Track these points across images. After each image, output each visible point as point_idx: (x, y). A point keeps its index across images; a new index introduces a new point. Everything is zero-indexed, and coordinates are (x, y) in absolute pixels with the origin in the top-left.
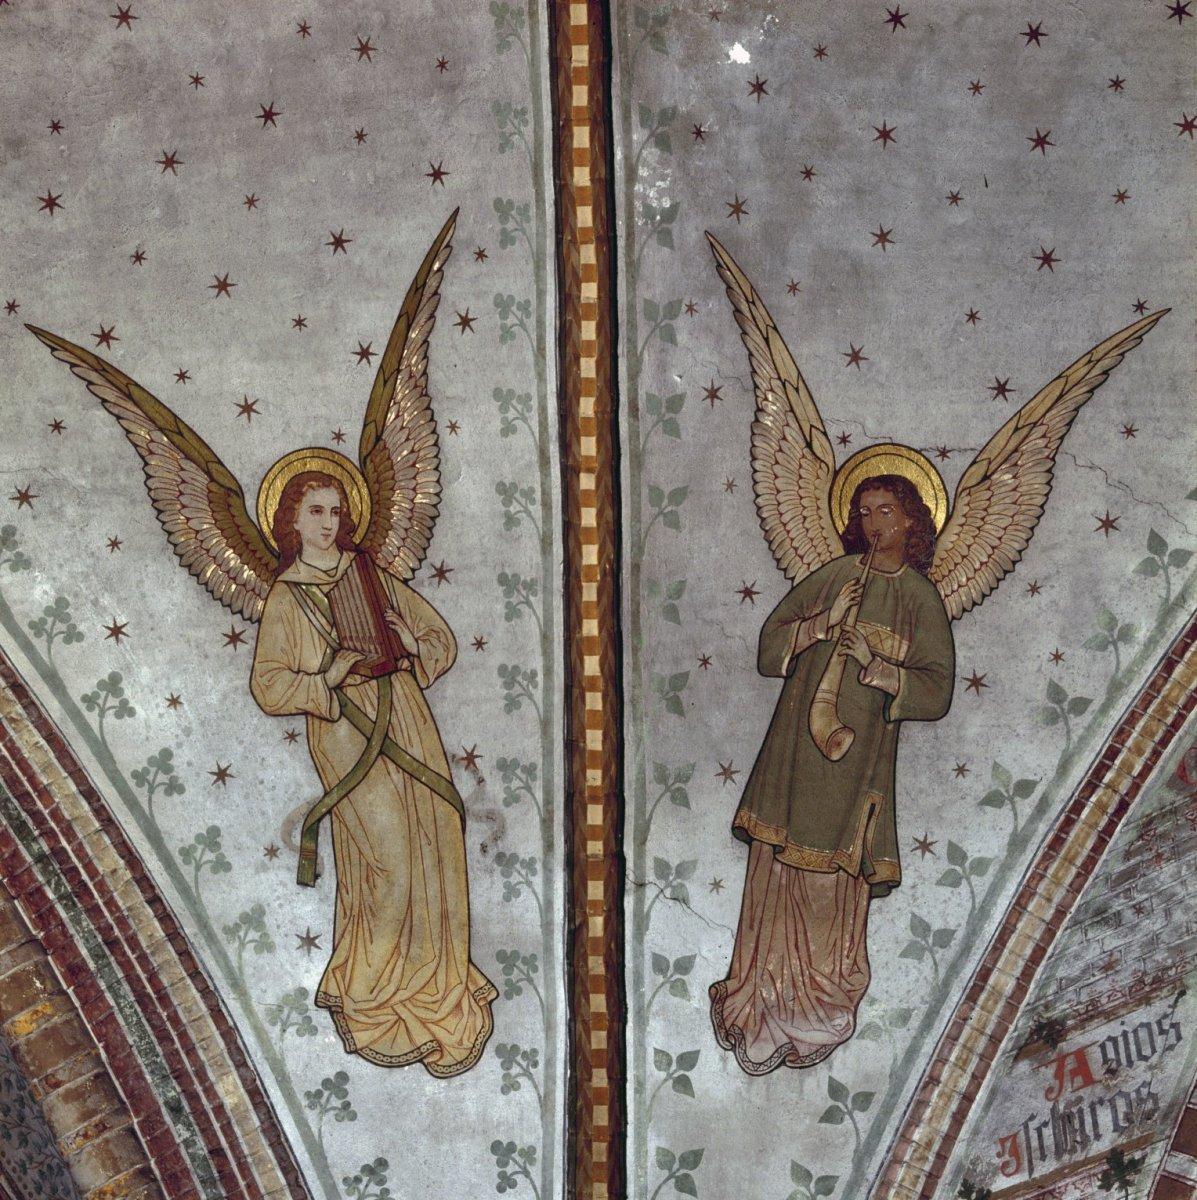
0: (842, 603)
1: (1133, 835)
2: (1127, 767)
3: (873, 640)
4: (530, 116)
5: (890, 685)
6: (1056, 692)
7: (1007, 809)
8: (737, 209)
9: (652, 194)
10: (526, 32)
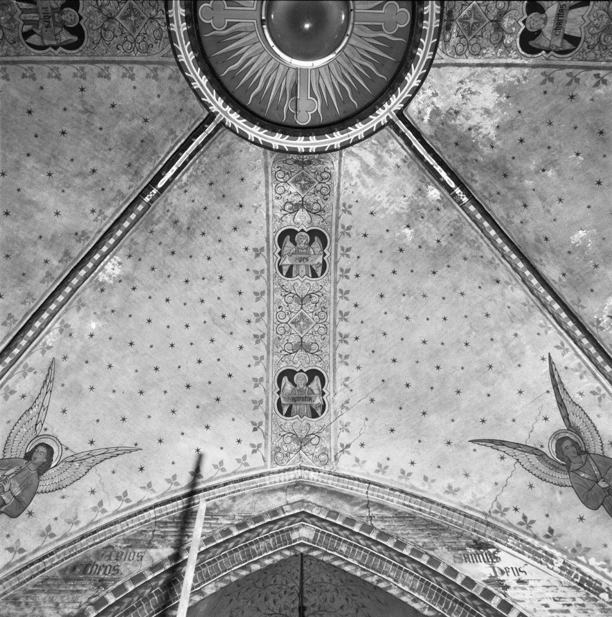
0: (12, 471)
1: (40, 580)
2: (53, 559)
3: (12, 486)
4: (35, 302)
5: (7, 501)
6: (49, 528)
7: (12, 555)
8: (65, 358)
9: (49, 340)
10: (51, 284)
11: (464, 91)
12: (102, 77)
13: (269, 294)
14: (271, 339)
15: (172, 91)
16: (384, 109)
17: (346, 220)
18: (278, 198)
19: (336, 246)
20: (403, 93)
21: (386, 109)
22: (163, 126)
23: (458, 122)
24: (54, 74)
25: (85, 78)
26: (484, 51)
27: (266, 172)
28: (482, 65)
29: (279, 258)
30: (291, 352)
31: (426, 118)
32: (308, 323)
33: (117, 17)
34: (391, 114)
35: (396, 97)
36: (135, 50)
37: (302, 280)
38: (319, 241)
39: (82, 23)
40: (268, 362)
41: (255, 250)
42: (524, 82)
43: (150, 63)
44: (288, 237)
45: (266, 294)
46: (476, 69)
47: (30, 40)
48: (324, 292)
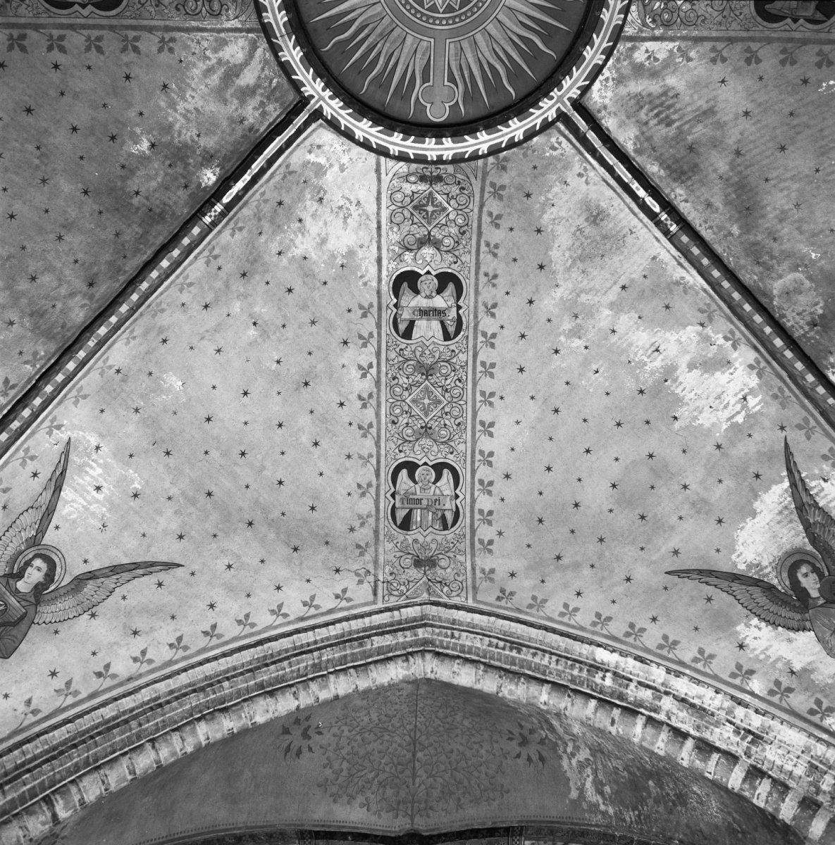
11: (348, 209)
16: (324, 90)
17: (149, 43)
19: (102, 27)
20: (346, 119)
21: (323, 94)
23: (308, 203)
26: (395, 229)
28: (379, 228)
31: (312, 157)
34: (317, 102)
35: (340, 108)
42: (360, 283)
46: (375, 221)
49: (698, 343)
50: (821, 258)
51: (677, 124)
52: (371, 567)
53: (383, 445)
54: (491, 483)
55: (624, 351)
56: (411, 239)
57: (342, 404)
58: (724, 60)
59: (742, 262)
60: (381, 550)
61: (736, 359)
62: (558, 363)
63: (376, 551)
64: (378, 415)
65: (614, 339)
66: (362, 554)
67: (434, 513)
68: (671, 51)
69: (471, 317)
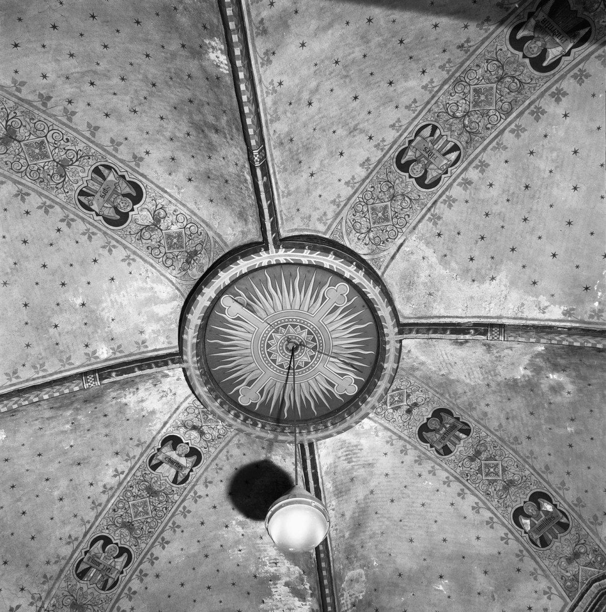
12: (366, 161)
13: (88, 139)
14: (36, 112)
15: (316, 209)
17: (120, 253)
18: (175, 211)
19: (100, 230)
20: (195, 373)
22: (298, 188)
24: (397, 125)
25: (376, 146)
26: (185, 414)
27: (203, 221)
28: (177, 409)
29: (120, 174)
30: (9, 123)
32: (34, 157)
33: (389, 203)
36: (361, 200)
37: (86, 179)
38: (114, 218)
39: (407, 174)
40: (10, 94)
41: (141, 159)
43: (345, 205)
44: (134, 194)
45: (90, 137)
47: (430, 128)
48: (59, 191)
49: (297, 578)
50: (377, 567)
51: (353, 464)
52: (44, 595)
53: (100, 519)
54: (146, 575)
55: (260, 551)
56: (190, 423)
57: (91, 484)
58: (392, 445)
59: (340, 556)
60: (57, 586)
61: (309, 601)
62: (224, 533)
63: (54, 585)
64: (108, 501)
65: (259, 541)
66: (44, 583)
67: (102, 576)
68: (371, 427)
69: (195, 480)
